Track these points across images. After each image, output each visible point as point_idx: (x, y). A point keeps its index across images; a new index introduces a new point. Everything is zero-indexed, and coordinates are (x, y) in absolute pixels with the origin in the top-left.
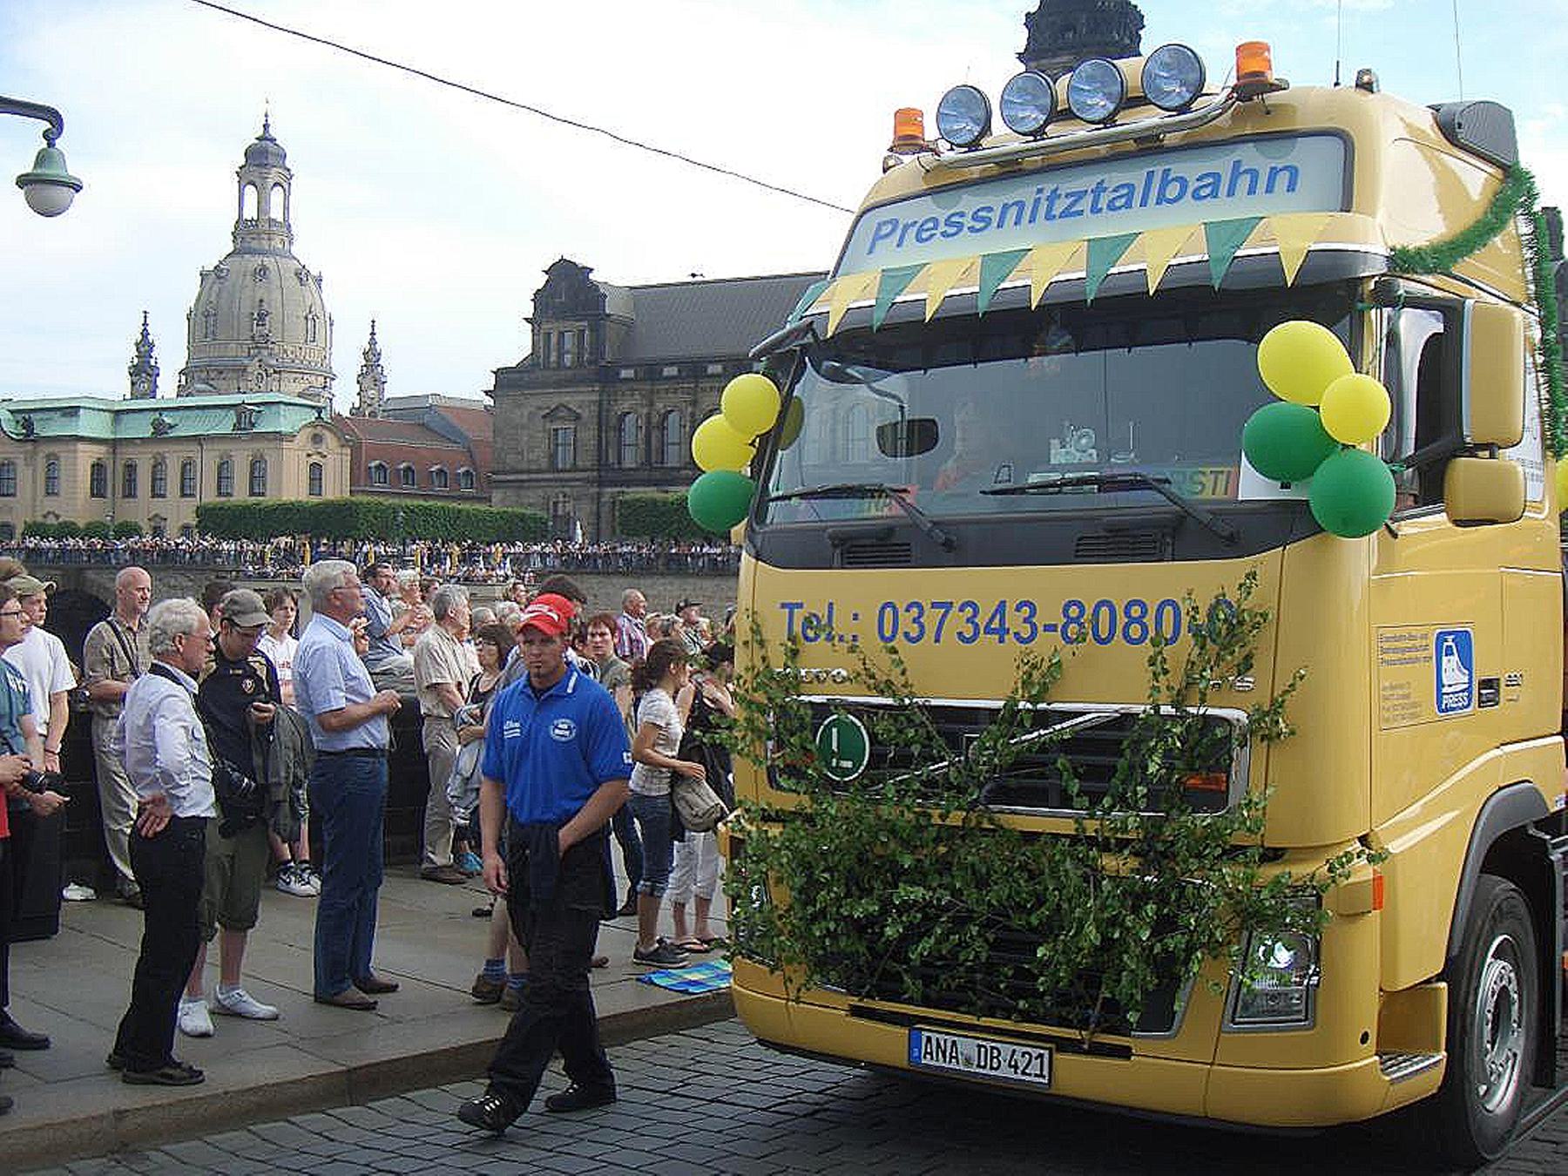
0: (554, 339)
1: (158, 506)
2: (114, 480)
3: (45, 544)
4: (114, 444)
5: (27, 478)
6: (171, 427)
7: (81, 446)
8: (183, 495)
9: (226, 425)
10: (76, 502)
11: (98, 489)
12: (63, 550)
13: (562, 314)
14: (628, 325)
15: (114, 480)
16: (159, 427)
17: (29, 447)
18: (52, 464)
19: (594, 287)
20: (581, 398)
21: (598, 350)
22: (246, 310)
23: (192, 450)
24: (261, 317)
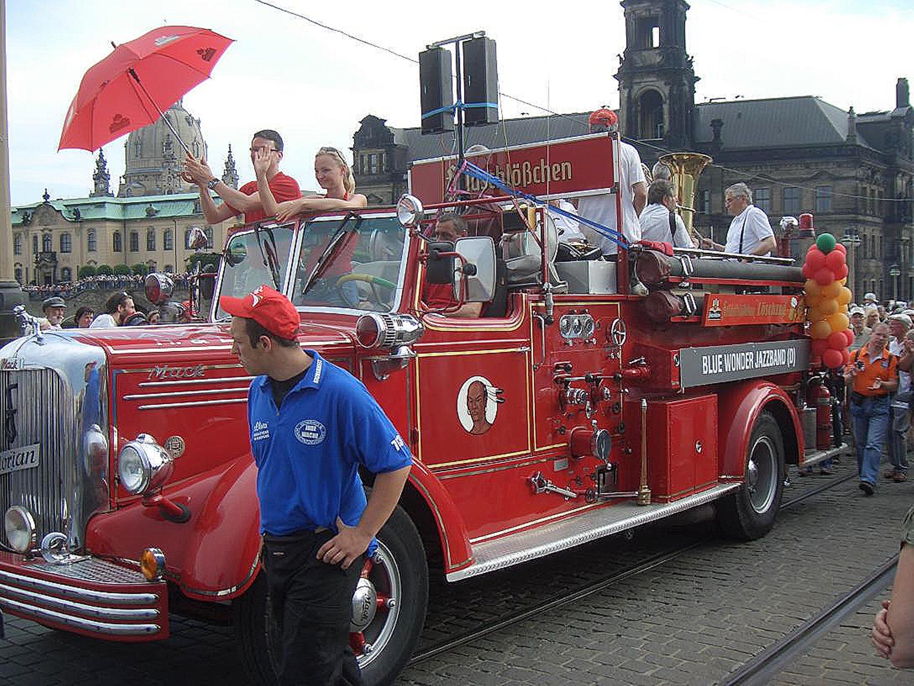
0: (366, 158)
1: (151, 255)
2: (126, 242)
3: (109, 279)
4: (124, 222)
5: (77, 242)
6: (157, 212)
7: (108, 224)
8: (165, 249)
9: (189, 210)
10: (105, 256)
11: (117, 248)
12: (119, 281)
13: (371, 145)
14: (405, 150)
15: (126, 242)
16: (151, 214)
17: (78, 225)
18: (91, 234)
19: (387, 130)
20: (380, 190)
21: (390, 161)
22: (159, 141)
23: (170, 225)
24: (168, 144)
